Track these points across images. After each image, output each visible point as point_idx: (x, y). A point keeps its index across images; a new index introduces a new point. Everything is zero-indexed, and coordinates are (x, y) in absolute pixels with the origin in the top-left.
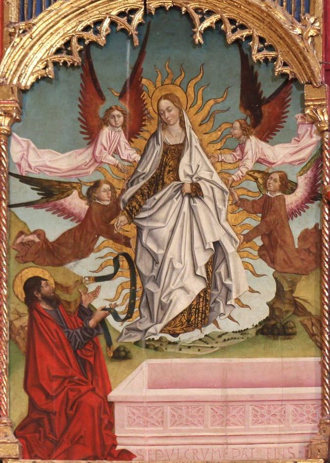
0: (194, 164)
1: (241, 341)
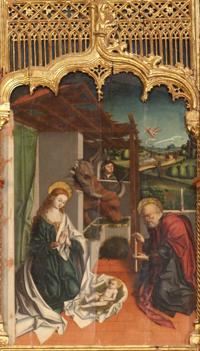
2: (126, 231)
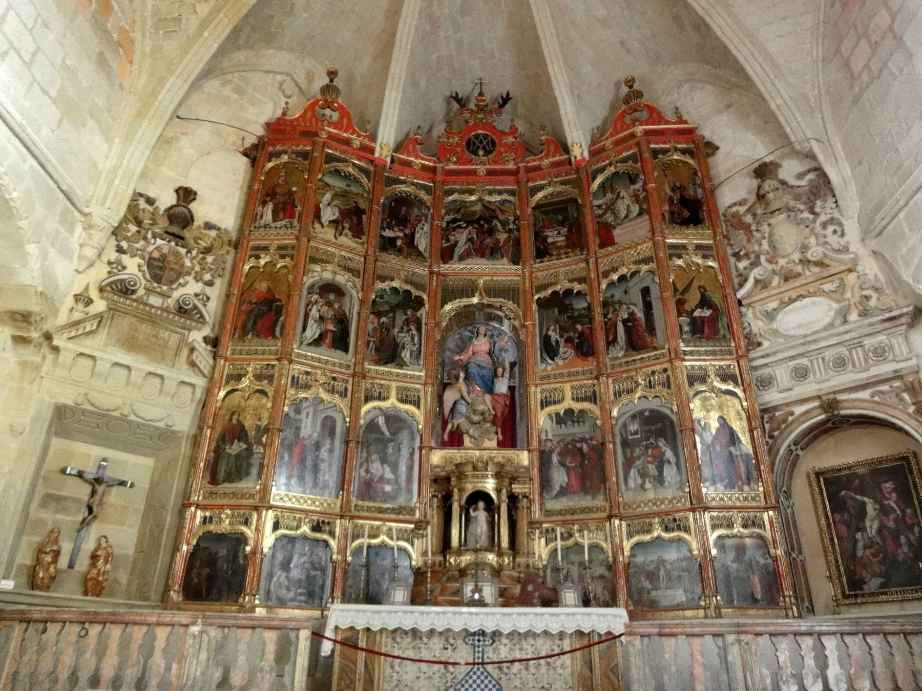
0: (623, 193)
1: (635, 218)
2: (572, 334)
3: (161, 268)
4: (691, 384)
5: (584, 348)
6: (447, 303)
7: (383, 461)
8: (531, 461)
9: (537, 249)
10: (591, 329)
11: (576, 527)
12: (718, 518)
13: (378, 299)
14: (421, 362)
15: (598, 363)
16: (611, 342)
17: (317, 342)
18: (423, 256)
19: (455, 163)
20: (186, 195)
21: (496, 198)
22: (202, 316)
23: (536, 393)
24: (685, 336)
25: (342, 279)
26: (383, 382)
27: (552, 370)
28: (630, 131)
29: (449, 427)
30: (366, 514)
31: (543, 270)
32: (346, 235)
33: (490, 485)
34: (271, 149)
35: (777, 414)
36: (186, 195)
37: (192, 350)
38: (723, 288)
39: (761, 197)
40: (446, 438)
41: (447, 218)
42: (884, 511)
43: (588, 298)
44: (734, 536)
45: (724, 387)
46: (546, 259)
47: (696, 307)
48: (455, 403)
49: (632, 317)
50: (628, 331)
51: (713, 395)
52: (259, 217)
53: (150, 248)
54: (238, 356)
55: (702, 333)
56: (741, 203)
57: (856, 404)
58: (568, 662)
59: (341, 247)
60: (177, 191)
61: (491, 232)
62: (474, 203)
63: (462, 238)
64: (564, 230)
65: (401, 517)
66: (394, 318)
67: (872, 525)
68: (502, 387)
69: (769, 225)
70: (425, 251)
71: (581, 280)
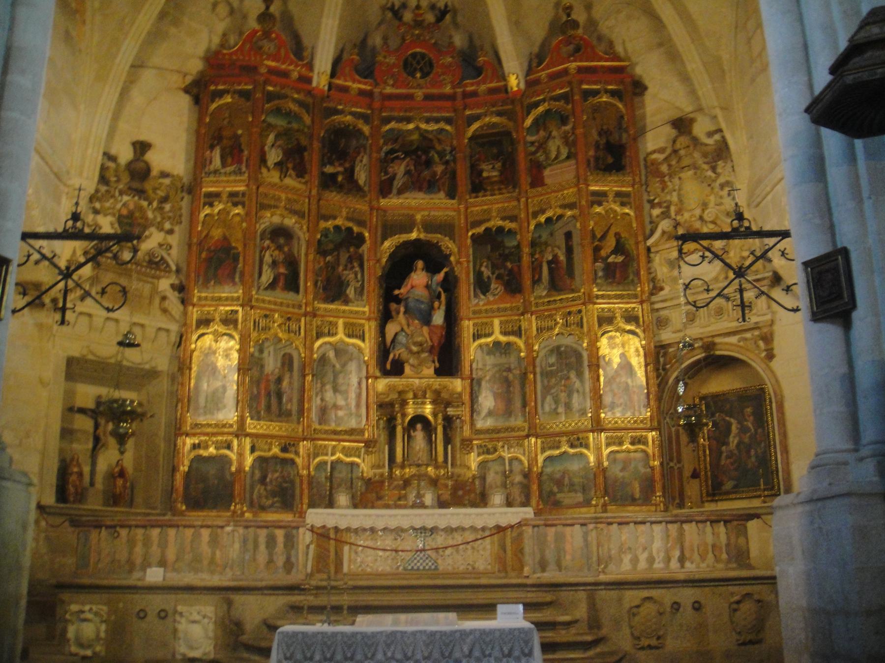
0: (554, 133)
2: (502, 271)
3: (131, 225)
4: (600, 325)
5: (513, 286)
6: (386, 239)
7: (336, 390)
8: (464, 388)
9: (473, 183)
10: (519, 267)
11: (500, 444)
12: (612, 437)
13: (323, 238)
14: (365, 297)
15: (524, 301)
16: (536, 281)
17: (272, 286)
18: (364, 192)
19: (393, 86)
20: (141, 147)
21: (432, 127)
22: (168, 265)
23: (467, 327)
24: (599, 281)
25: (290, 222)
26: (331, 319)
27: (484, 305)
28: (566, 66)
29: (391, 356)
30: (324, 436)
31: (480, 204)
32: (290, 176)
33: (428, 410)
34: (212, 88)
35: (671, 350)
36: (141, 147)
37: (164, 298)
38: (636, 236)
39: (675, 152)
40: (388, 367)
41: (385, 149)
42: (743, 430)
43: (518, 237)
44: (623, 451)
45: (628, 327)
46: (481, 194)
47: (612, 253)
48: (396, 334)
49: (555, 260)
50: (551, 271)
51: (618, 334)
52: (208, 162)
53: (119, 206)
54: (203, 302)
55: (614, 277)
56: (661, 150)
57: (727, 347)
58: (489, 547)
59: (286, 188)
60: (134, 144)
61: (429, 163)
62: (410, 132)
63: (400, 169)
64: (498, 165)
65: (353, 437)
66: (338, 255)
67: (733, 441)
68: (438, 318)
69: (680, 178)
70: (365, 185)
71: (513, 218)
